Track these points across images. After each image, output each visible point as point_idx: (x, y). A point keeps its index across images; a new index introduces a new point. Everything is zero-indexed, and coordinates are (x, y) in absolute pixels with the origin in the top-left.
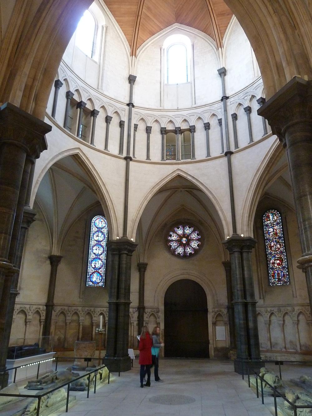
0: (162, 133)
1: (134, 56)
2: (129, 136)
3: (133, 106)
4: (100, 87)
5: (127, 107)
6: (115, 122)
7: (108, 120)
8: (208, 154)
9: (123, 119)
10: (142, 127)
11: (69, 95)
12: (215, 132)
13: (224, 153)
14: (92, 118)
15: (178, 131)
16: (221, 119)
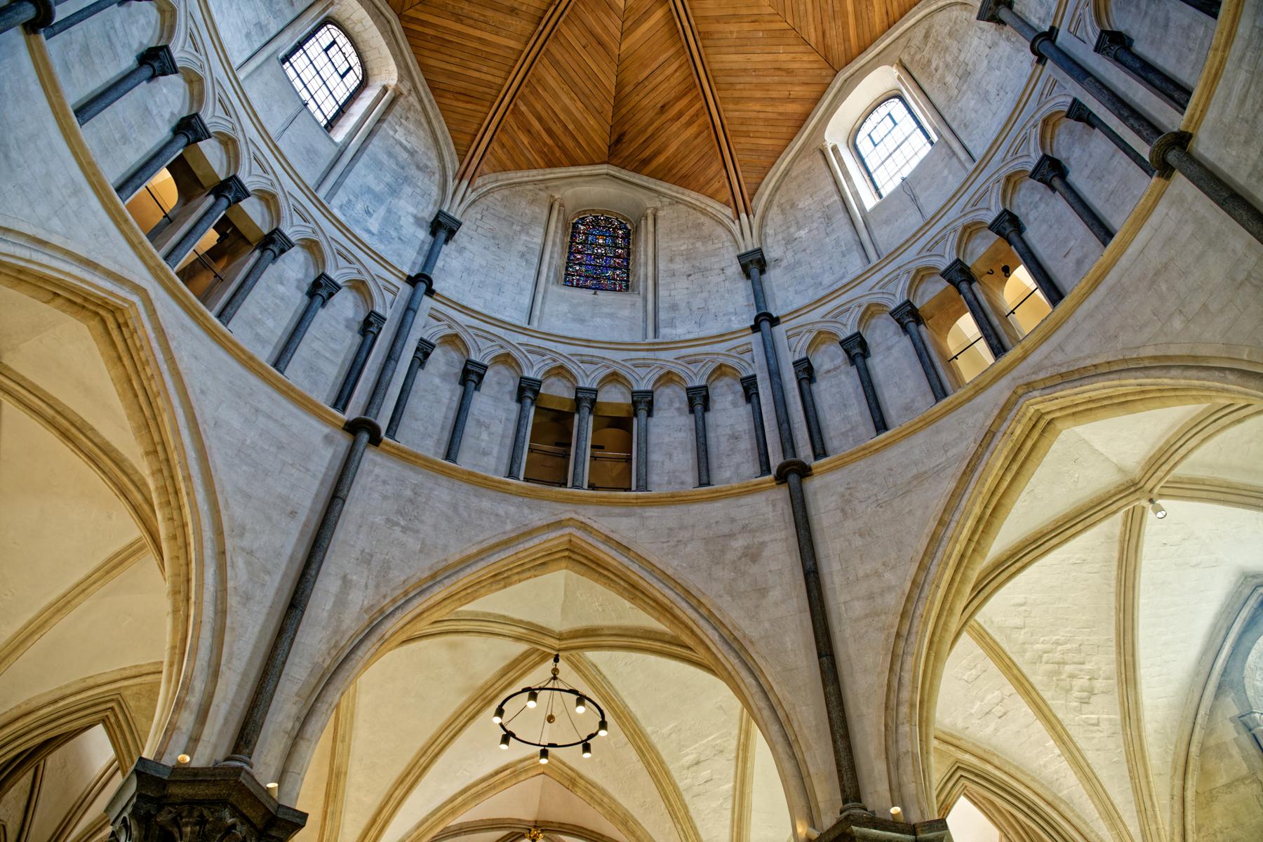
0: (520, 400)
1: (465, 183)
2: (392, 356)
3: (430, 292)
5: (406, 289)
7: (320, 289)
9: (378, 310)
13: (769, 472)
14: (257, 253)
15: (585, 399)
16: (755, 376)
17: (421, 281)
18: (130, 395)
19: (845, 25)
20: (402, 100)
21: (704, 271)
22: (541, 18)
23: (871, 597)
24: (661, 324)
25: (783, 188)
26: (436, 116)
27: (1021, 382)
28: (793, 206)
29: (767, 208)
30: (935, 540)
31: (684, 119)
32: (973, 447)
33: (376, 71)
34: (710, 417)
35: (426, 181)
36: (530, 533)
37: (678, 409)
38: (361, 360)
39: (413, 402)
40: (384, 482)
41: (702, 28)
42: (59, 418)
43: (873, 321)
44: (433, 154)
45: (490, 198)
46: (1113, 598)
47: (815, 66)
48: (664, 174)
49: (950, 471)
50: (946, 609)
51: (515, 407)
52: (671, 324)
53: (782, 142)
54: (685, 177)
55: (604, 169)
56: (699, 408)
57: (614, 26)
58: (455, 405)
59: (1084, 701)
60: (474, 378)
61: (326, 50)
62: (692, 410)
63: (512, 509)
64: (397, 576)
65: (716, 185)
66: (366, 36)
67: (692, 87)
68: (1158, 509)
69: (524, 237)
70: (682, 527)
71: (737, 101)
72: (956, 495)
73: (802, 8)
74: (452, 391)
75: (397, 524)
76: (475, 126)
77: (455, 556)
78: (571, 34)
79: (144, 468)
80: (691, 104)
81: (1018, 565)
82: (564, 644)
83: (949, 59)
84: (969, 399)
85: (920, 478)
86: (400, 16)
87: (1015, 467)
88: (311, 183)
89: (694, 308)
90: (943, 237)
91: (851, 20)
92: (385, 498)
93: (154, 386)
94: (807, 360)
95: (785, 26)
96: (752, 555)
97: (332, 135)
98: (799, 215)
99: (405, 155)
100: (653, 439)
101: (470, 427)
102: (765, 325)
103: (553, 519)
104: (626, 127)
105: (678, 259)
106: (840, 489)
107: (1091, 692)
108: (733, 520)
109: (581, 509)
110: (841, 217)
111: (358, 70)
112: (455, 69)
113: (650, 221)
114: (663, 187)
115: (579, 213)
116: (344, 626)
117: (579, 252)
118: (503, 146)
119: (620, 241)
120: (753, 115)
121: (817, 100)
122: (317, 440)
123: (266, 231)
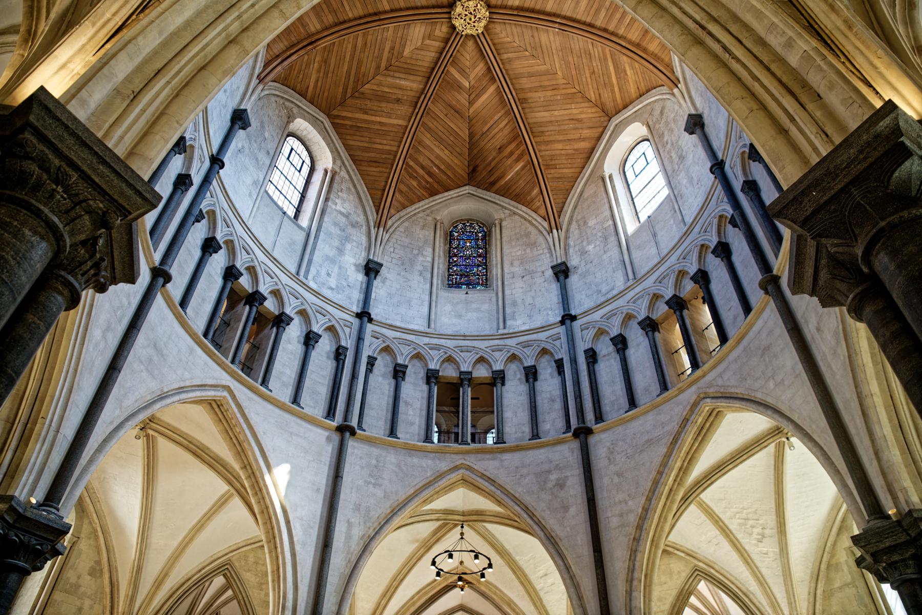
0: (428, 382)
3: (370, 320)
4: (302, 273)
5: (356, 322)
6: (325, 346)
7: (310, 340)
8: (535, 435)
9: (343, 343)
10: (383, 366)
11: (231, 274)
12: (549, 384)
14: (275, 329)
15: (466, 378)
16: (562, 359)
17: (364, 315)
18: (228, 439)
19: (613, 92)
20: (337, 177)
21: (531, 273)
22: (417, 103)
23: (621, 515)
24: (507, 317)
25: (579, 207)
26: (358, 180)
27: (701, 391)
28: (585, 223)
29: (570, 223)
30: (656, 483)
31: (514, 157)
32: (676, 427)
33: (318, 158)
34: (538, 385)
35: (358, 234)
36: (441, 476)
37: (520, 379)
38: (338, 380)
39: (369, 397)
40: (361, 458)
41: (521, 96)
42: (191, 445)
43: (631, 322)
44: (360, 211)
45: (397, 233)
46: (772, 486)
47: (597, 115)
48: (504, 192)
49: (664, 441)
50: (662, 518)
51: (425, 388)
52: (514, 318)
53: (578, 170)
54: (516, 195)
55: (467, 189)
56: (531, 380)
57: (463, 99)
58: (392, 394)
59: (760, 541)
60: (401, 375)
61: (288, 159)
62: (527, 381)
63: (430, 462)
64: (374, 515)
65: (538, 204)
66: (310, 137)
67: (516, 136)
68: (791, 446)
69: (421, 258)
70: (523, 466)
71: (548, 143)
72: (668, 456)
73: (584, 80)
74: (389, 384)
75: (370, 483)
76: (383, 184)
77: (402, 497)
78: (437, 109)
79: (236, 466)
80: (518, 147)
81: (709, 482)
82: (466, 518)
83: (674, 139)
84: (676, 396)
85: (650, 442)
86: (329, 116)
87: (700, 438)
88: (294, 271)
89: (527, 304)
90: (668, 275)
91: (616, 89)
92: (362, 468)
93: (241, 437)
94: (592, 350)
95: (574, 90)
96: (561, 485)
97: (299, 222)
98: (589, 232)
99: (344, 219)
101: (402, 407)
102: (568, 322)
103: (452, 465)
104: (478, 162)
105: (516, 263)
106: (608, 444)
107: (764, 537)
108: (551, 462)
109: (466, 457)
110: (613, 238)
111: (308, 161)
112: (366, 145)
113: (498, 227)
114: (504, 201)
115: (453, 223)
116: (352, 549)
117: (456, 256)
118: (401, 192)
119: (480, 243)
120: (558, 152)
121: (599, 138)
122: (323, 440)
123: (277, 313)
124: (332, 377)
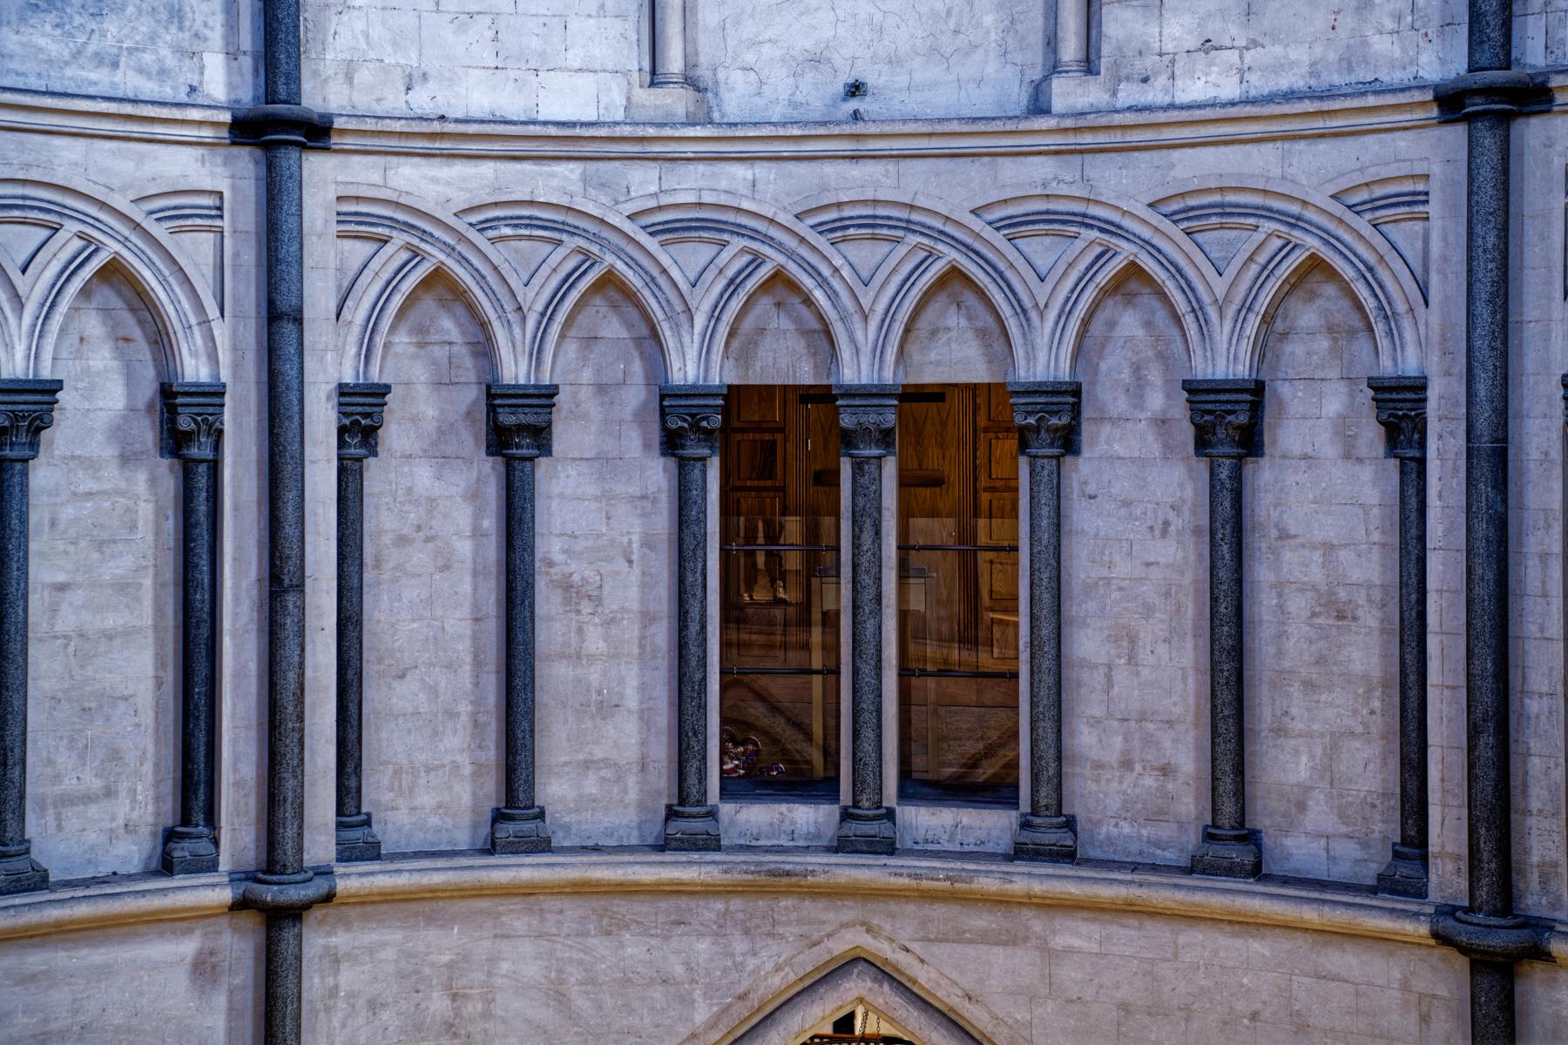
0: (671, 443)
34: (1263, 476)
39: (378, 611)
40: (374, 1006)
51: (657, 474)
63: (703, 947)
74: (474, 495)
100: (1081, 565)
124: (169, 573)
